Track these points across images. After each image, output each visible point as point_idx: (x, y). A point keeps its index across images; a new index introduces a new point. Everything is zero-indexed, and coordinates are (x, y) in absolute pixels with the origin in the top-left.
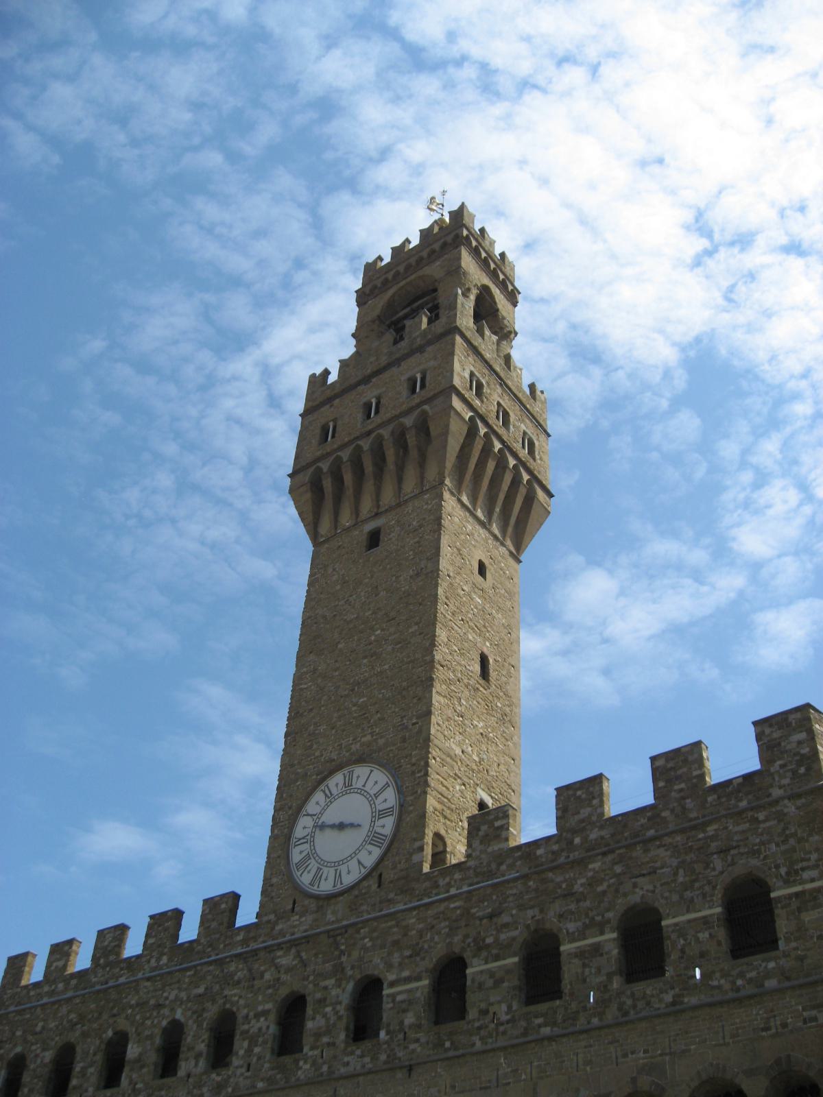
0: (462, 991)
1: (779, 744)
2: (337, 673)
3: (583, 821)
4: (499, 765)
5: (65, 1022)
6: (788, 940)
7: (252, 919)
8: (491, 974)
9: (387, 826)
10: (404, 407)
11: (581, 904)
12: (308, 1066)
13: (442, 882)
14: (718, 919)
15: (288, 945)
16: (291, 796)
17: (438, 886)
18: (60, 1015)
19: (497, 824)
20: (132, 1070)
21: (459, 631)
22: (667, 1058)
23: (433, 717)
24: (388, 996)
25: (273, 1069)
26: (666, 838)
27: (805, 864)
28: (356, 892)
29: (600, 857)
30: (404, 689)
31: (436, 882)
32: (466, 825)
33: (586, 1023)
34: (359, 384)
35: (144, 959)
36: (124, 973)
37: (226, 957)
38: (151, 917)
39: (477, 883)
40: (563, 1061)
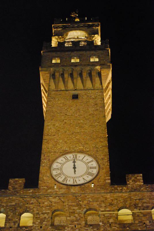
9: (95, 171)
19: (138, 178)
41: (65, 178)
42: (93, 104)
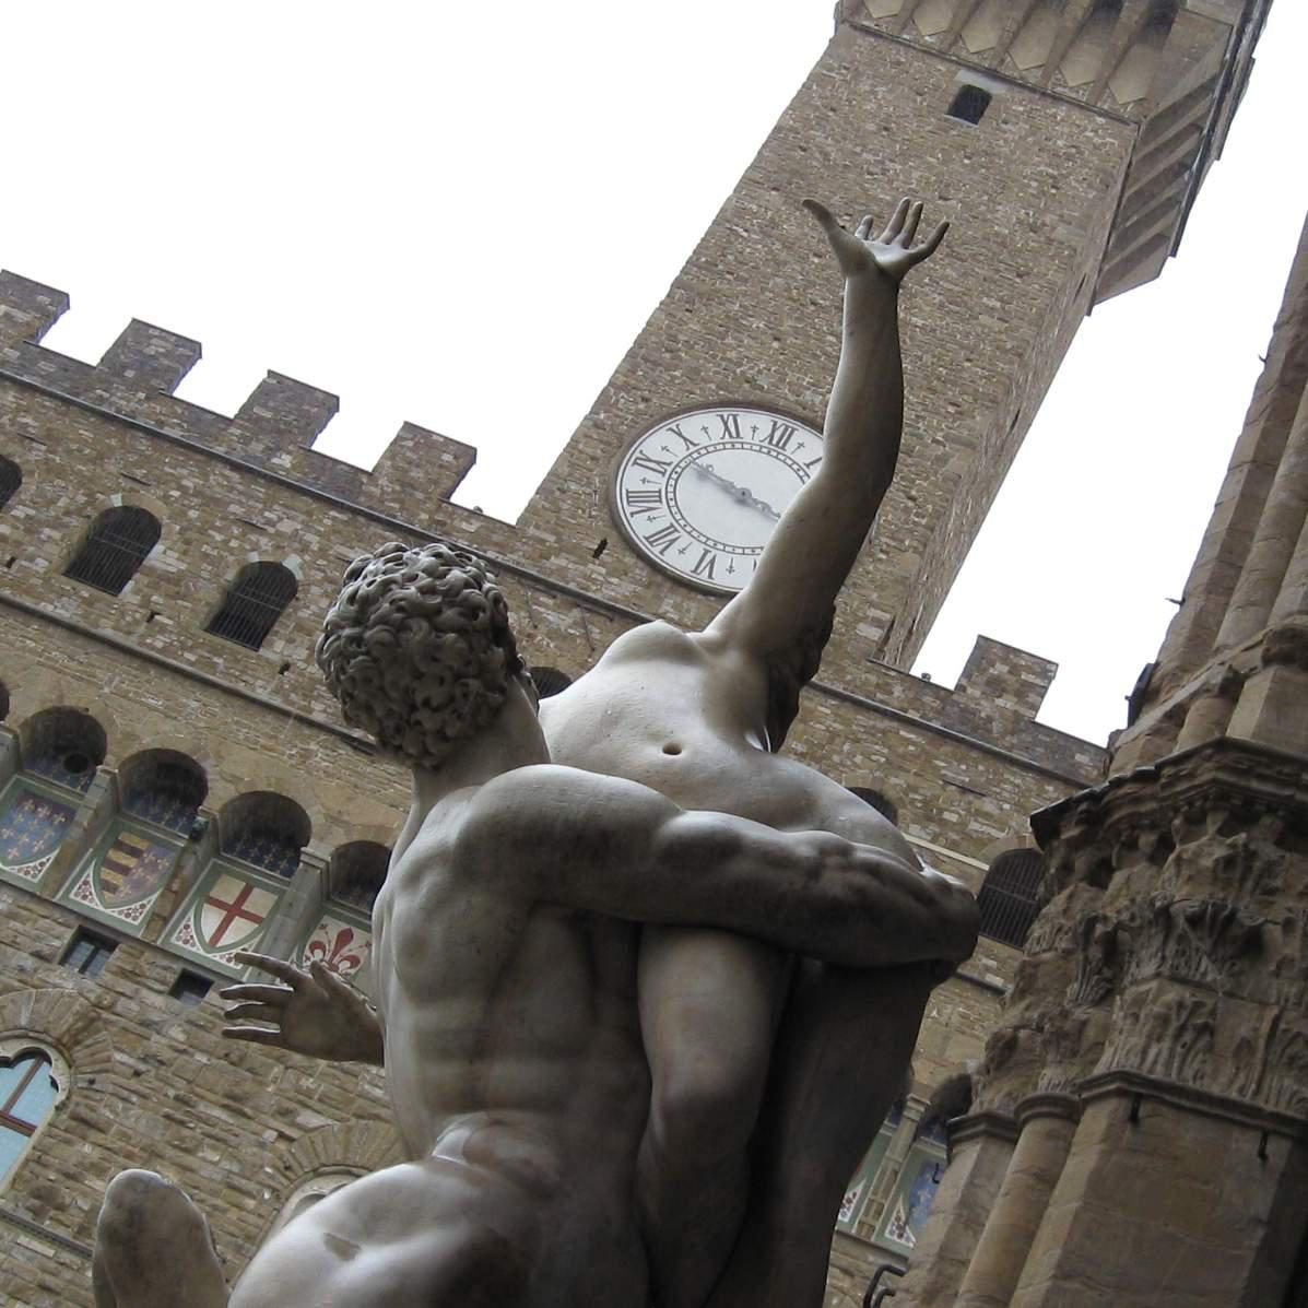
2: (816, 260)
41: (672, 526)
42: (1034, 184)
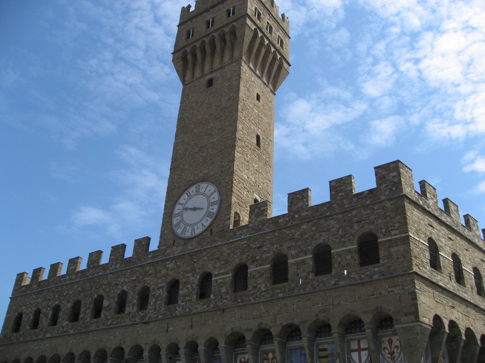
0: (246, 278)
1: (385, 177)
2: (193, 143)
3: (299, 208)
4: (263, 183)
5: (76, 291)
6: (384, 259)
7: (156, 248)
8: (258, 272)
9: (215, 209)
10: (225, 23)
11: (297, 243)
12: (180, 309)
13: (238, 233)
14: (355, 250)
15: (172, 259)
16: (173, 196)
17: (236, 235)
18: (74, 288)
19: (262, 209)
20: (106, 311)
21: (247, 125)
22: (331, 306)
23: (235, 162)
24: (214, 280)
25: (166, 310)
26: (334, 216)
27: (393, 228)
28: (201, 237)
29: (306, 223)
30: (223, 150)
31: (235, 233)
32: (249, 209)
33: (298, 292)
34: (204, 12)
35: (109, 265)
36: (101, 271)
37: (145, 264)
38: (112, 247)
39: (253, 234)
40: (288, 307)
42: (227, 89)
